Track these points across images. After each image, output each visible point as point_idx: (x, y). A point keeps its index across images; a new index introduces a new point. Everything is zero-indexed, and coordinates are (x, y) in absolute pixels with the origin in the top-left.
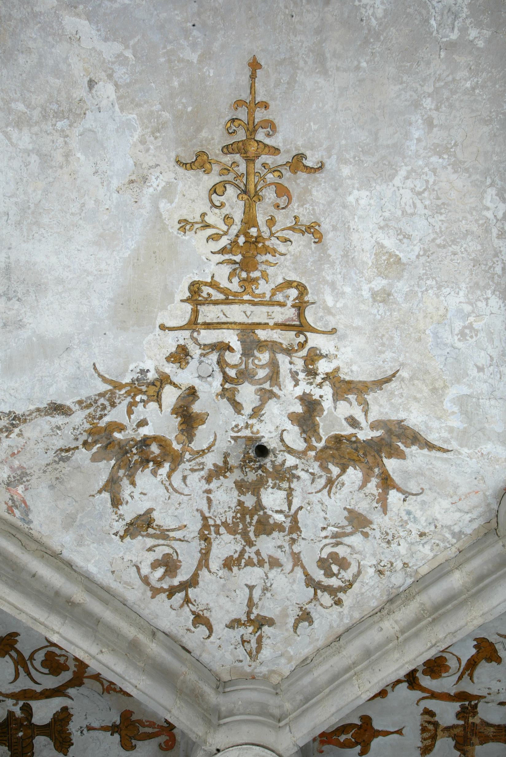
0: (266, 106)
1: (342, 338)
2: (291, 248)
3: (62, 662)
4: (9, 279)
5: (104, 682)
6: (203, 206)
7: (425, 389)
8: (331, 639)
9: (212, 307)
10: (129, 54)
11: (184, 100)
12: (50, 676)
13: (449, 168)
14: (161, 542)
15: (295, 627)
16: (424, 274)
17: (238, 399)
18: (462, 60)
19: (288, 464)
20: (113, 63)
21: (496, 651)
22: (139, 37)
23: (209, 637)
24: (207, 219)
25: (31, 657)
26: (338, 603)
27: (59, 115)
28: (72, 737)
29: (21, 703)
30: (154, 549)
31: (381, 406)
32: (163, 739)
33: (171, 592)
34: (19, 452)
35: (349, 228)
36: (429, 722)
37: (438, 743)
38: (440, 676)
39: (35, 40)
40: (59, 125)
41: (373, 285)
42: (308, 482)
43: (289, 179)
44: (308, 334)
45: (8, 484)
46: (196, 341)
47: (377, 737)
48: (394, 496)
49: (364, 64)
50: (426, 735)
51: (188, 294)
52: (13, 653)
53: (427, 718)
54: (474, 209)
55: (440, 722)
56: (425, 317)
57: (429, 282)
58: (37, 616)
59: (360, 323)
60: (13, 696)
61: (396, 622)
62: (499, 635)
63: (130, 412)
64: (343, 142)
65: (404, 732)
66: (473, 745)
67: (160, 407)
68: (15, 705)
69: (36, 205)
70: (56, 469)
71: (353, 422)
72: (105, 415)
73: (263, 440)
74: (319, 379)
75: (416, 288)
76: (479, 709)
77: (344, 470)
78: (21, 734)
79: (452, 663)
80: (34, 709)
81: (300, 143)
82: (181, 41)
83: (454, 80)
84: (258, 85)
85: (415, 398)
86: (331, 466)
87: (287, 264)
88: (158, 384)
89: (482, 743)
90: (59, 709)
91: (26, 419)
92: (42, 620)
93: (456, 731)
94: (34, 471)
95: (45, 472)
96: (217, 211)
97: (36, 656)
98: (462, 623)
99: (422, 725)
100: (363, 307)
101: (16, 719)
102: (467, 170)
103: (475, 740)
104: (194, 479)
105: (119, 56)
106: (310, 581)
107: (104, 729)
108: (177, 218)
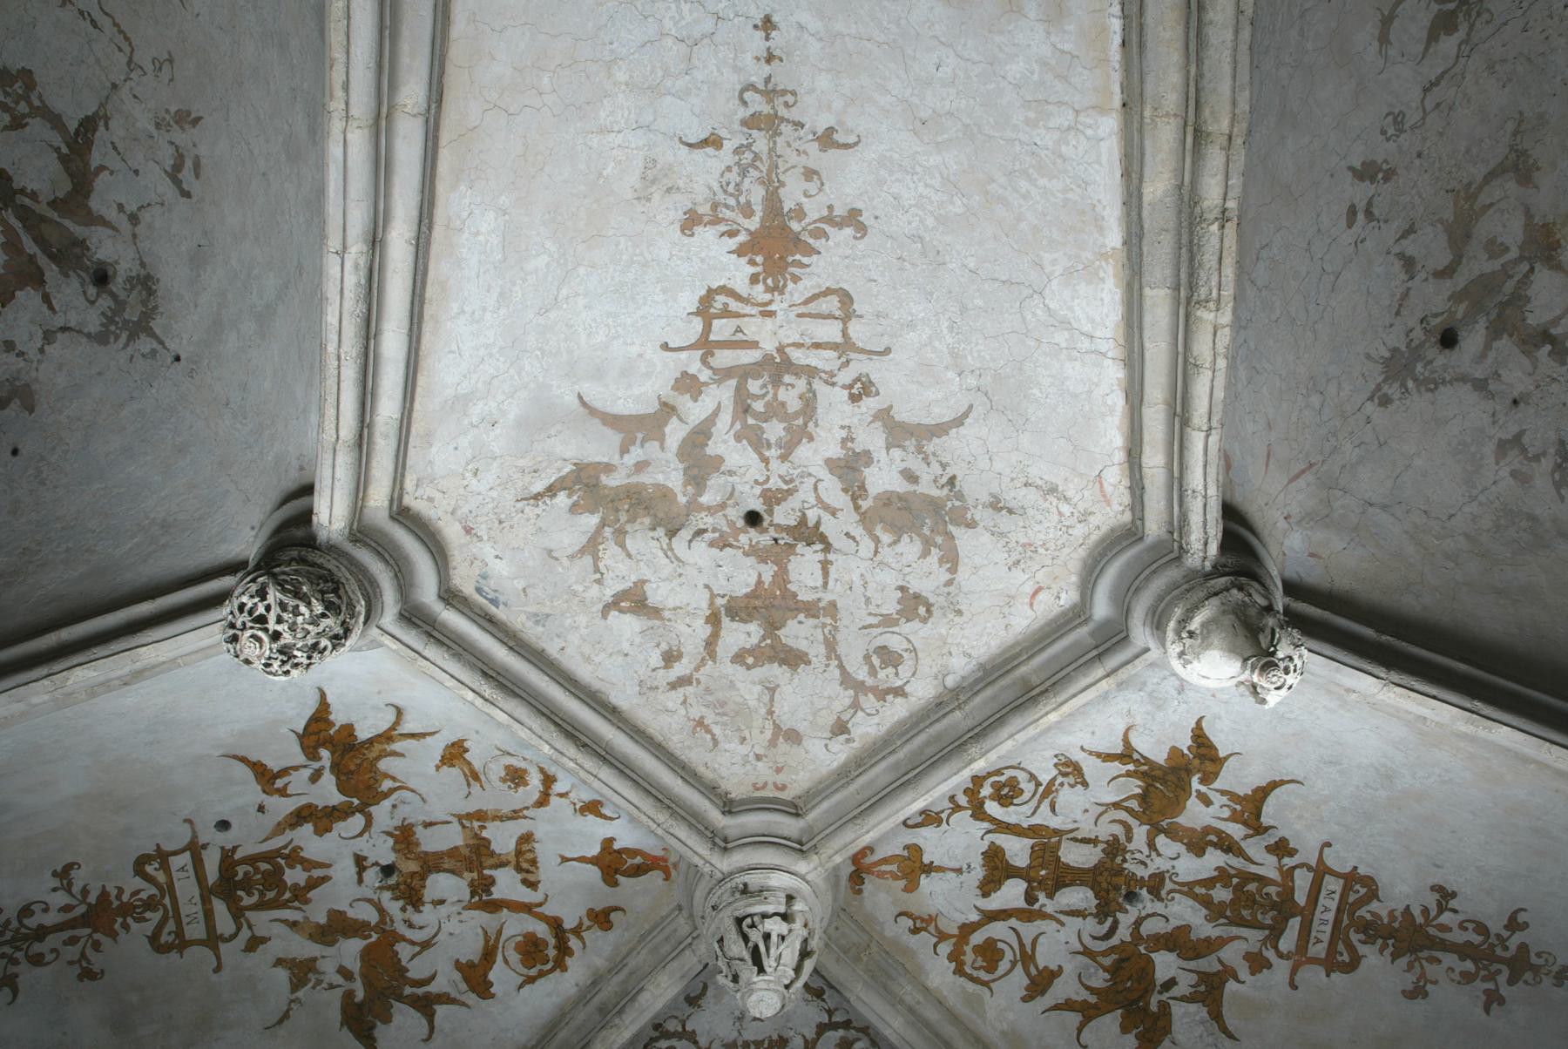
3: (980, 959)
5: (933, 931)
21: (466, 980)
25: (1014, 964)
28: (982, 862)
29: (1037, 906)
36: (528, 871)
37: (512, 846)
38: (525, 936)
47: (593, 857)
50: (529, 856)
52: (1033, 972)
53: (531, 878)
55: (514, 872)
60: (1043, 916)
65: (559, 860)
66: (467, 846)
68: (1044, 905)
76: (468, 891)
78: (1043, 873)
79: (514, 957)
80: (1023, 898)
89: (456, 848)
90: (993, 895)
93: (491, 861)
97: (1008, 966)
99: (537, 868)
101: (1045, 890)
103: (466, 852)
107: (941, 869)
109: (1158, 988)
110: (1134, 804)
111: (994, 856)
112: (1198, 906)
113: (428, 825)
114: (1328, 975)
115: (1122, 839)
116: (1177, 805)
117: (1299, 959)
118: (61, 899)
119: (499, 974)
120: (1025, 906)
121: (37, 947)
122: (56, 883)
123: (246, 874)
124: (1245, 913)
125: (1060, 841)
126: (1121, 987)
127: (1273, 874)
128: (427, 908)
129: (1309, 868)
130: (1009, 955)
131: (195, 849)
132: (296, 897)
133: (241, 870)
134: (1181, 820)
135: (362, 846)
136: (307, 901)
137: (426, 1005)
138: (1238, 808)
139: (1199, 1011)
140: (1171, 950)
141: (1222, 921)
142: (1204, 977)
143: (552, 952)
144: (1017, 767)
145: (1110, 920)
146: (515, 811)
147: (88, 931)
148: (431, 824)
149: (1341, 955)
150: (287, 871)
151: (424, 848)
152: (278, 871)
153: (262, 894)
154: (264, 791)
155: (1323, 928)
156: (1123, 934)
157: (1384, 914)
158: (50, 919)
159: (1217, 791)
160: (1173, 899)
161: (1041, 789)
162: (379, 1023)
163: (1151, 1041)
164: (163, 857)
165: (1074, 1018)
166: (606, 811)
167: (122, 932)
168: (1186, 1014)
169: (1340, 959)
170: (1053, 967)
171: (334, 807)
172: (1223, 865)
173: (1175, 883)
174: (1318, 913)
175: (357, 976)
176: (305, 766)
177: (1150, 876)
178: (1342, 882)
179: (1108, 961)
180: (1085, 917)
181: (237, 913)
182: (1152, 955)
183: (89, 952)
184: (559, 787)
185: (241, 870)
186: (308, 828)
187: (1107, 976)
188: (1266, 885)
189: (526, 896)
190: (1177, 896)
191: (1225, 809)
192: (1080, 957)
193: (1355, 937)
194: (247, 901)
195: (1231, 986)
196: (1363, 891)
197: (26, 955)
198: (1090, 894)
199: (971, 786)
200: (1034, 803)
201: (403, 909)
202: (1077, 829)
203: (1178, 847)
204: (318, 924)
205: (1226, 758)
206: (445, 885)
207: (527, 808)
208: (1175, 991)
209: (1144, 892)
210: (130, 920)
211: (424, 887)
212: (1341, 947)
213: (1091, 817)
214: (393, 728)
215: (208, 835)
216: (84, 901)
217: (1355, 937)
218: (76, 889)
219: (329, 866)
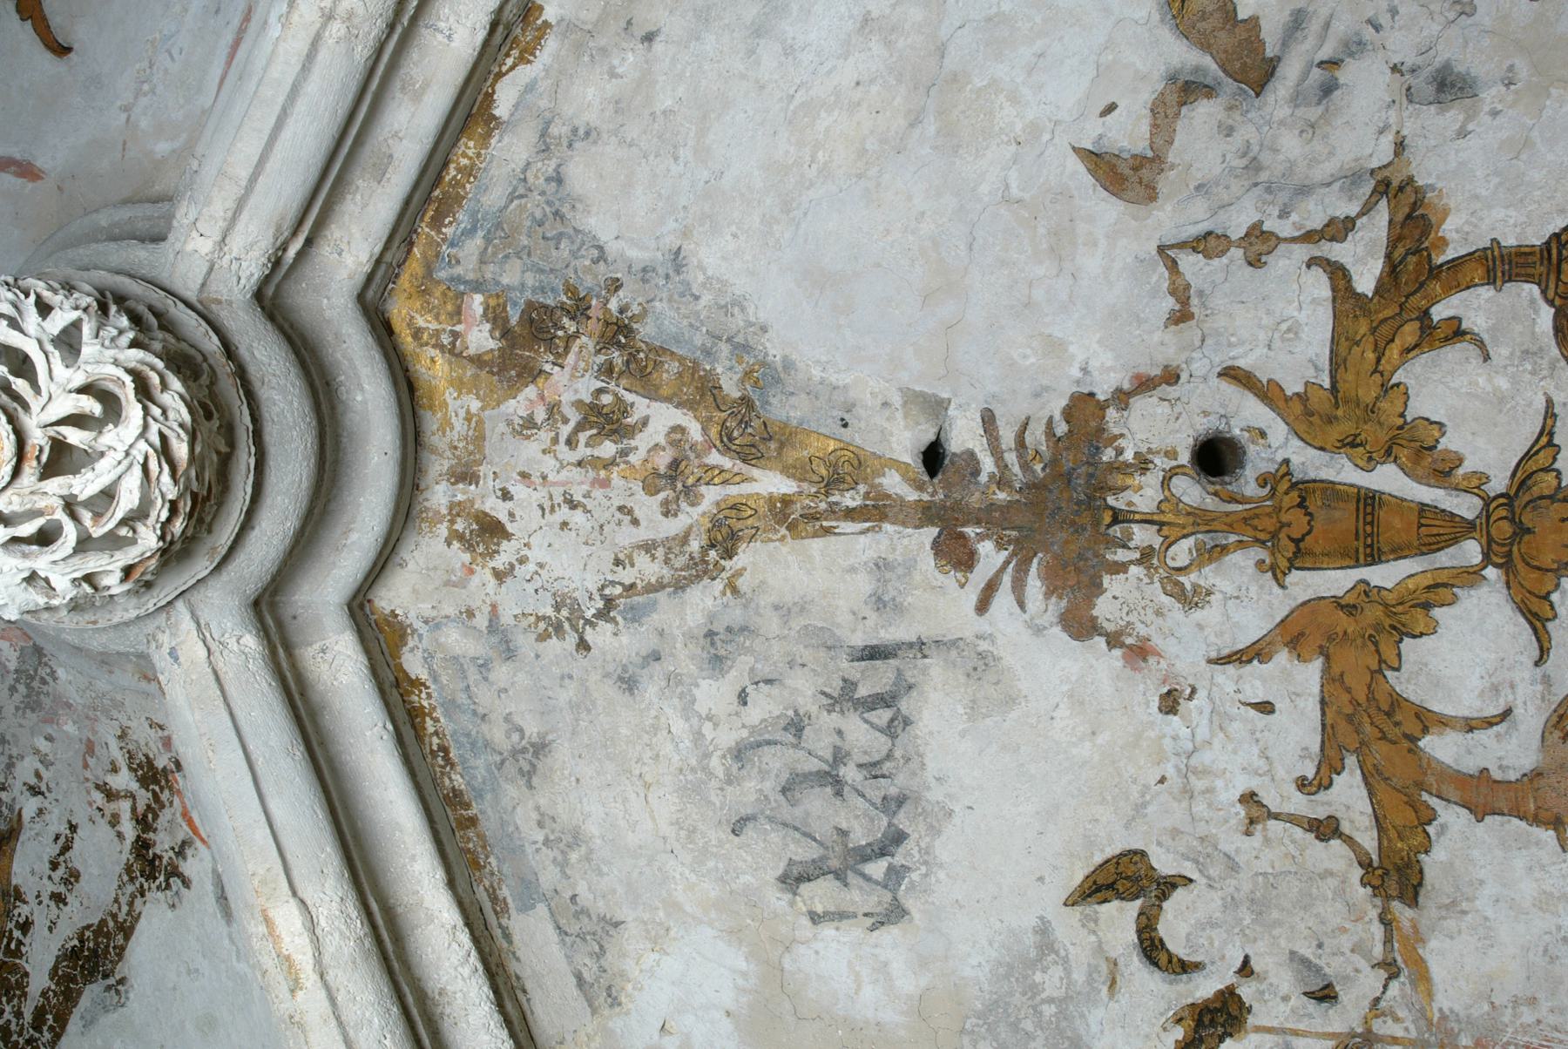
34: (86, 766)
91: (132, 880)
94: (21, 726)
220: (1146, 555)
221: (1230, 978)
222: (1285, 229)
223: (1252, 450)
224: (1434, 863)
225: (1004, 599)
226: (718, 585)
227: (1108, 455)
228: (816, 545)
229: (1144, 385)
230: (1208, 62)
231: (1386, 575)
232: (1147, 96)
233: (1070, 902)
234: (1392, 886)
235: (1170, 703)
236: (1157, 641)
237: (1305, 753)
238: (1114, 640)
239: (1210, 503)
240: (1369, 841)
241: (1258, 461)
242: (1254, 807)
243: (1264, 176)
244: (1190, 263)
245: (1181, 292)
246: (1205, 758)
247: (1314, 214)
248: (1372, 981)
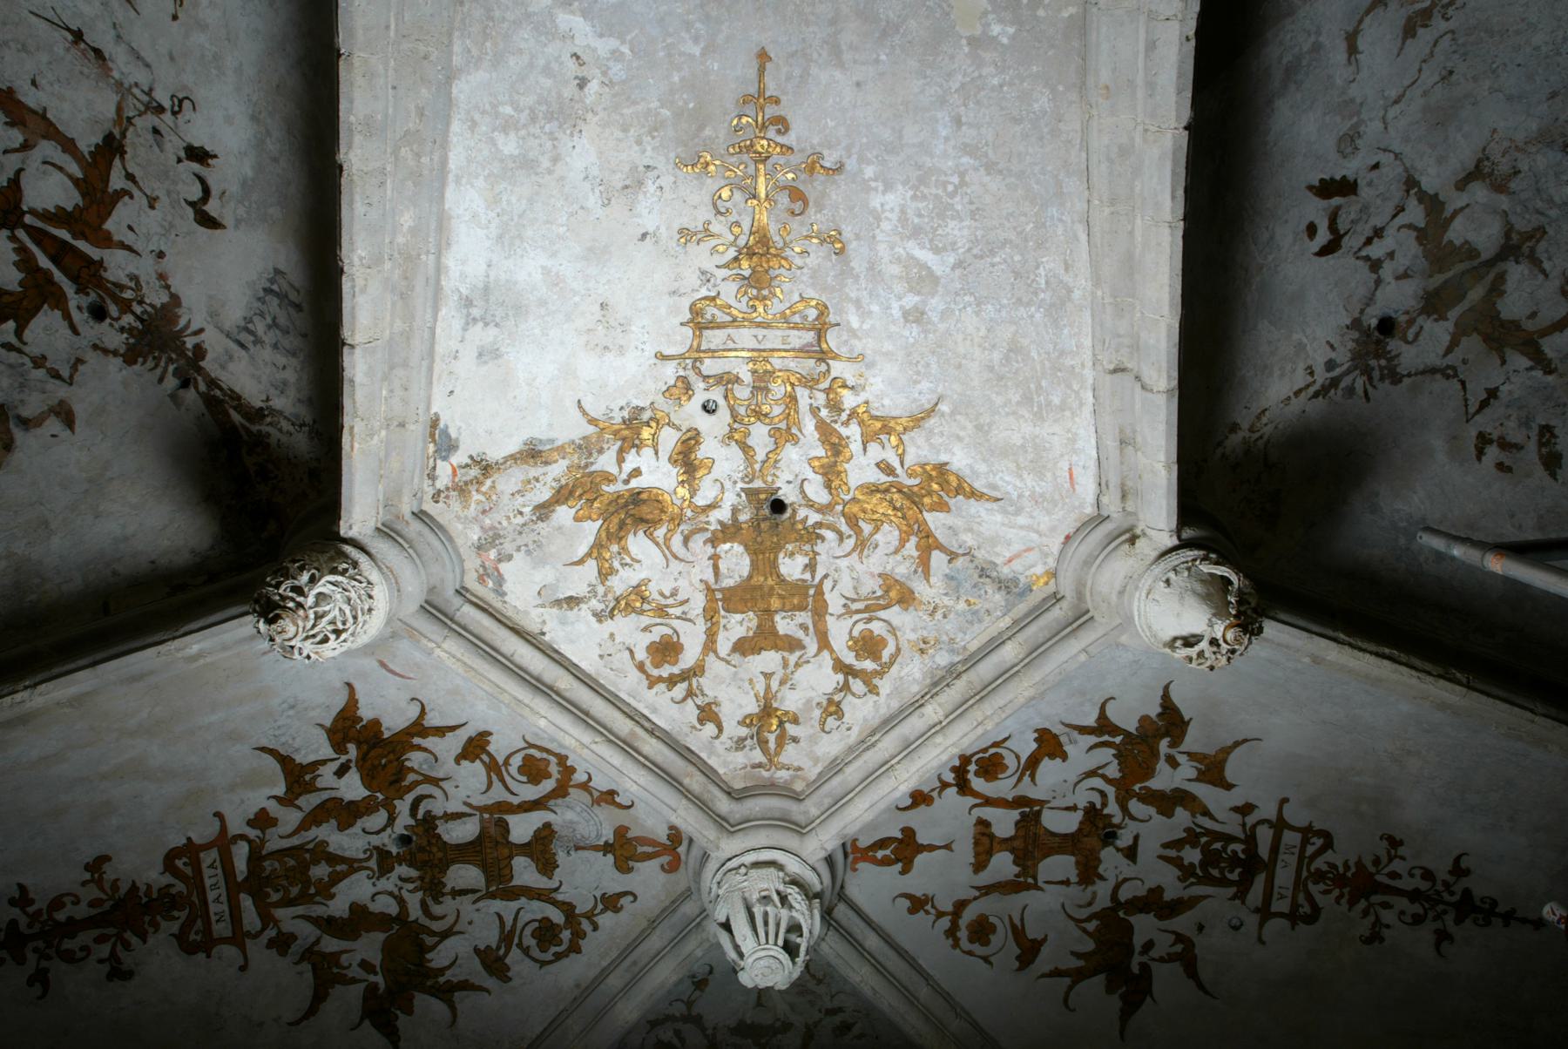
0: (777, 102)
1: (870, 366)
2: (808, 260)
4: (487, 301)
6: (706, 213)
7: (970, 426)
8: (865, 734)
9: (717, 332)
10: (625, 49)
11: (685, 96)
12: (529, 785)
13: (982, 169)
14: (659, 620)
15: (823, 723)
16: (962, 289)
17: (750, 442)
18: (988, 56)
19: (810, 522)
20: (608, 59)
21: (1060, 745)
22: (637, 31)
23: (717, 737)
24: (711, 227)
25: (507, 762)
26: (873, 690)
27: (550, 117)
30: (653, 629)
31: (918, 447)
32: (665, 859)
33: (672, 681)
35: (874, 237)
36: (983, 834)
39: (526, 40)
40: (547, 128)
41: (904, 302)
42: (835, 544)
43: (804, 182)
44: (830, 362)
45: (479, 548)
46: (699, 373)
48: (937, 558)
49: (883, 57)
51: (689, 316)
52: (484, 757)
54: (1011, 215)
56: (965, 339)
57: (967, 298)
58: (521, 698)
59: (891, 348)
61: (940, 705)
62: (1063, 724)
63: (621, 460)
64: (865, 140)
65: (953, 846)
67: (656, 453)
69: (520, 216)
70: (533, 530)
71: (885, 468)
72: (592, 463)
73: (780, 493)
74: (844, 416)
75: (953, 306)
77: (877, 529)
79: (1010, 761)
81: (815, 141)
82: (683, 34)
83: (980, 76)
84: (767, 79)
85: (959, 439)
86: (861, 523)
87: (805, 279)
88: (653, 424)
90: (540, 825)
92: (526, 701)
93: (1017, 844)
95: (520, 533)
96: (722, 218)
97: (512, 761)
98: (1011, 696)
100: (893, 328)
102: (1000, 172)
104: (698, 542)
105: (613, 52)
106: (840, 666)
108: (676, 227)
109: (353, 765)
110: (429, 941)
111: (547, 865)
112: (339, 853)
113: (1067, 883)
114: (189, 839)
115: (430, 901)
116: (388, 949)
117: (224, 842)
118: (1388, 916)
119: (1027, 746)
120: (505, 817)
121: (1424, 886)
122: (1386, 932)
123: (1231, 871)
124: (292, 862)
125: (487, 888)
126: (391, 756)
127: (281, 913)
128: (1082, 804)
129: (249, 934)
130: (513, 770)
131: (1265, 912)
132: (1198, 836)
133: (1234, 876)
134: (380, 937)
135: (1127, 869)
136: (1187, 830)
137: (1104, 726)
138: (335, 970)
139: (302, 758)
140: (351, 802)
141: (311, 846)
142: (311, 788)
143: (972, 768)
144: (543, 964)
145: (420, 815)
146: (986, 894)
147: (1379, 878)
148: (1061, 883)
149: (185, 864)
150: (1196, 862)
151: (1073, 859)
152: (1204, 864)
153: (1224, 848)
154: (1194, 945)
155: (213, 881)
156: (403, 806)
157: (164, 924)
158: (1402, 903)
159: (360, 981)
160: (365, 852)
161: (516, 940)
162: (1155, 719)
163: (348, 719)
164: (1293, 917)
165: (433, 720)
166: (907, 903)
167: (1351, 863)
168: (317, 751)
169: (185, 860)
170: (465, 763)
171: (1141, 911)
172: (329, 903)
173: (367, 868)
174: (223, 891)
175: (1163, 757)
176: (1154, 960)
177: (392, 869)
178: (215, 935)
179: (411, 777)
180: (446, 814)
181: (1250, 839)
182: (368, 793)
183: (1384, 860)
184: (945, 922)
185: (1234, 876)
186: (1168, 896)
187: (408, 764)
188: (282, 899)
189: (988, 813)
190: (362, 856)
191: (346, 964)
192: (441, 775)
193: (180, 887)
194: (1238, 847)
195: (280, 790)
196: (192, 937)
197: (1434, 885)
198: (446, 838)
199: (581, 942)
200: (520, 925)
201: (1104, 805)
202: (474, 902)
203: (376, 907)
204: (1185, 808)
205: (362, 1020)
206: (1060, 822)
207: (975, 898)
208: (335, 766)
209: (394, 850)
210: (1341, 870)
211: (1081, 823)
212: (188, 871)
213: (464, 919)
214: (1075, 983)
215: (1252, 920)
216: (1371, 905)
217: (180, 887)
218: (1372, 918)
219: (1160, 857)
220: (141, 302)
221: (186, 163)
222: (27, 360)
223: (84, 305)
224: (97, 139)
225: (194, 327)
226: (271, 403)
227: (132, 341)
228: (237, 389)
229: (106, 351)
230: (12, 426)
231: (63, 234)
232: (39, 431)
233: (224, 227)
234: (116, 144)
235: (161, 255)
236: (154, 276)
237: (125, 204)
238: (168, 287)
239: (108, 301)
240: (117, 162)
241: (84, 301)
242: (152, 203)
243: (21, 380)
244: (65, 373)
245: (74, 368)
246: (159, 230)
247: (13, 357)
248: (138, 121)
